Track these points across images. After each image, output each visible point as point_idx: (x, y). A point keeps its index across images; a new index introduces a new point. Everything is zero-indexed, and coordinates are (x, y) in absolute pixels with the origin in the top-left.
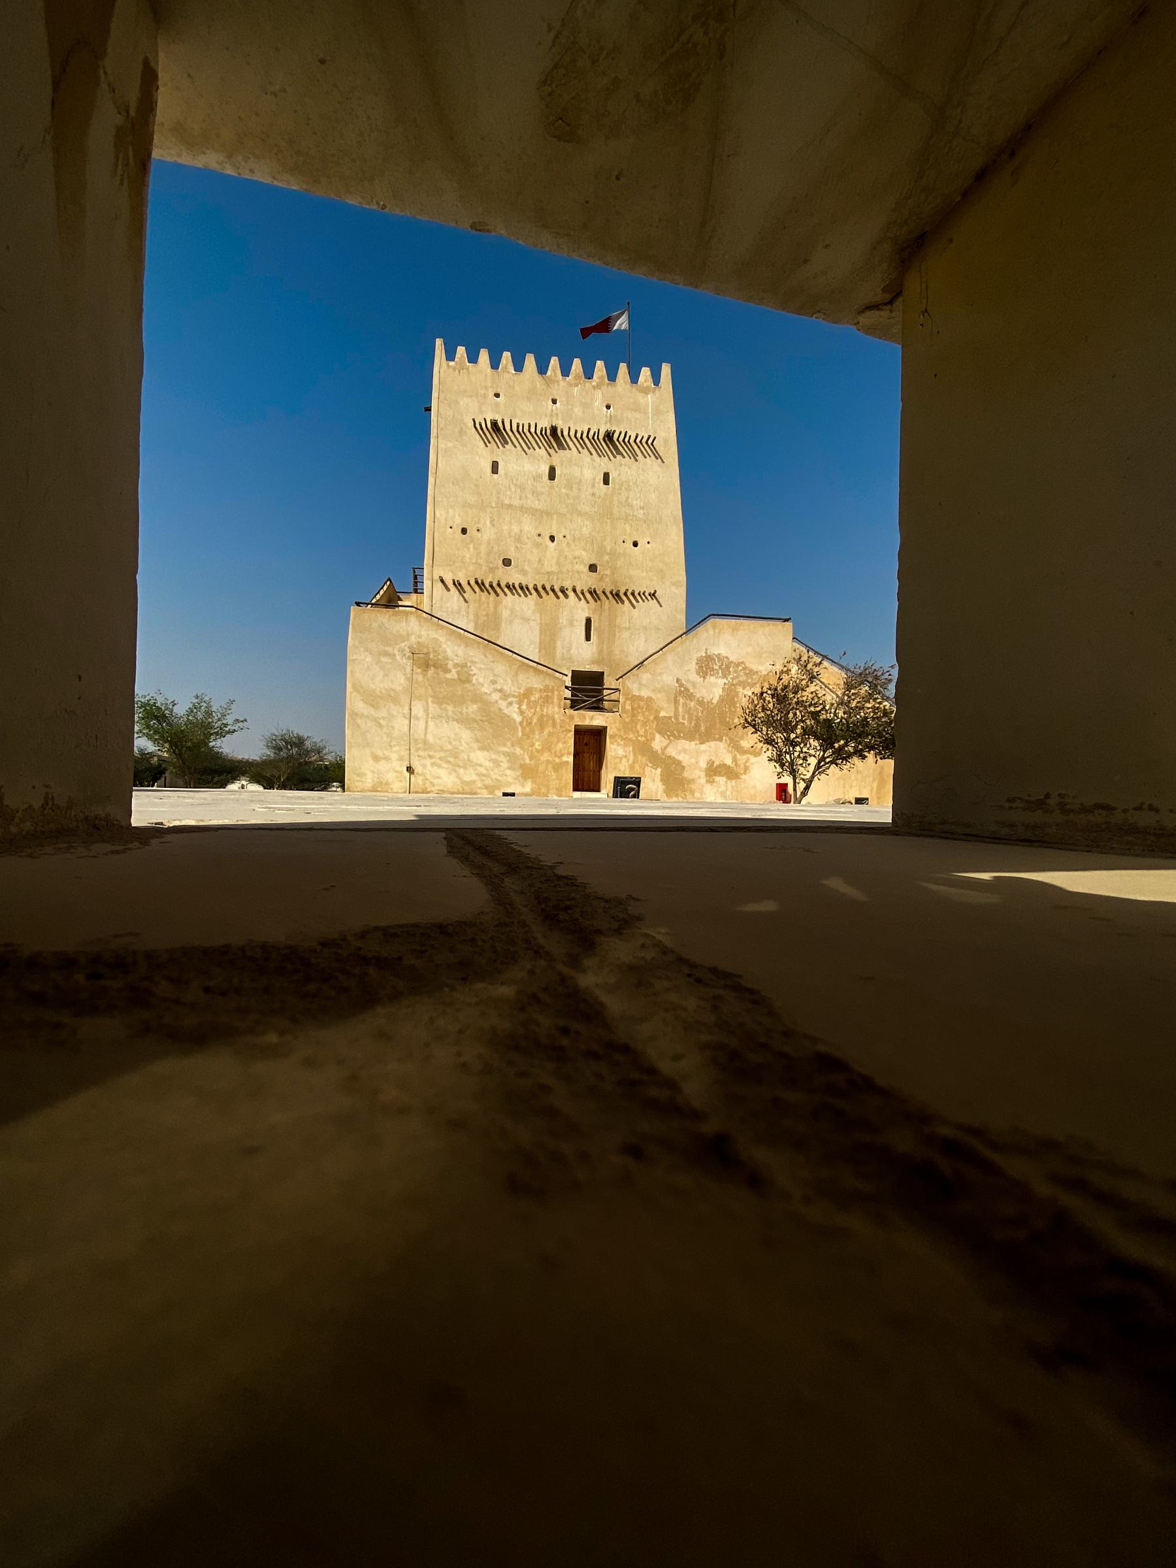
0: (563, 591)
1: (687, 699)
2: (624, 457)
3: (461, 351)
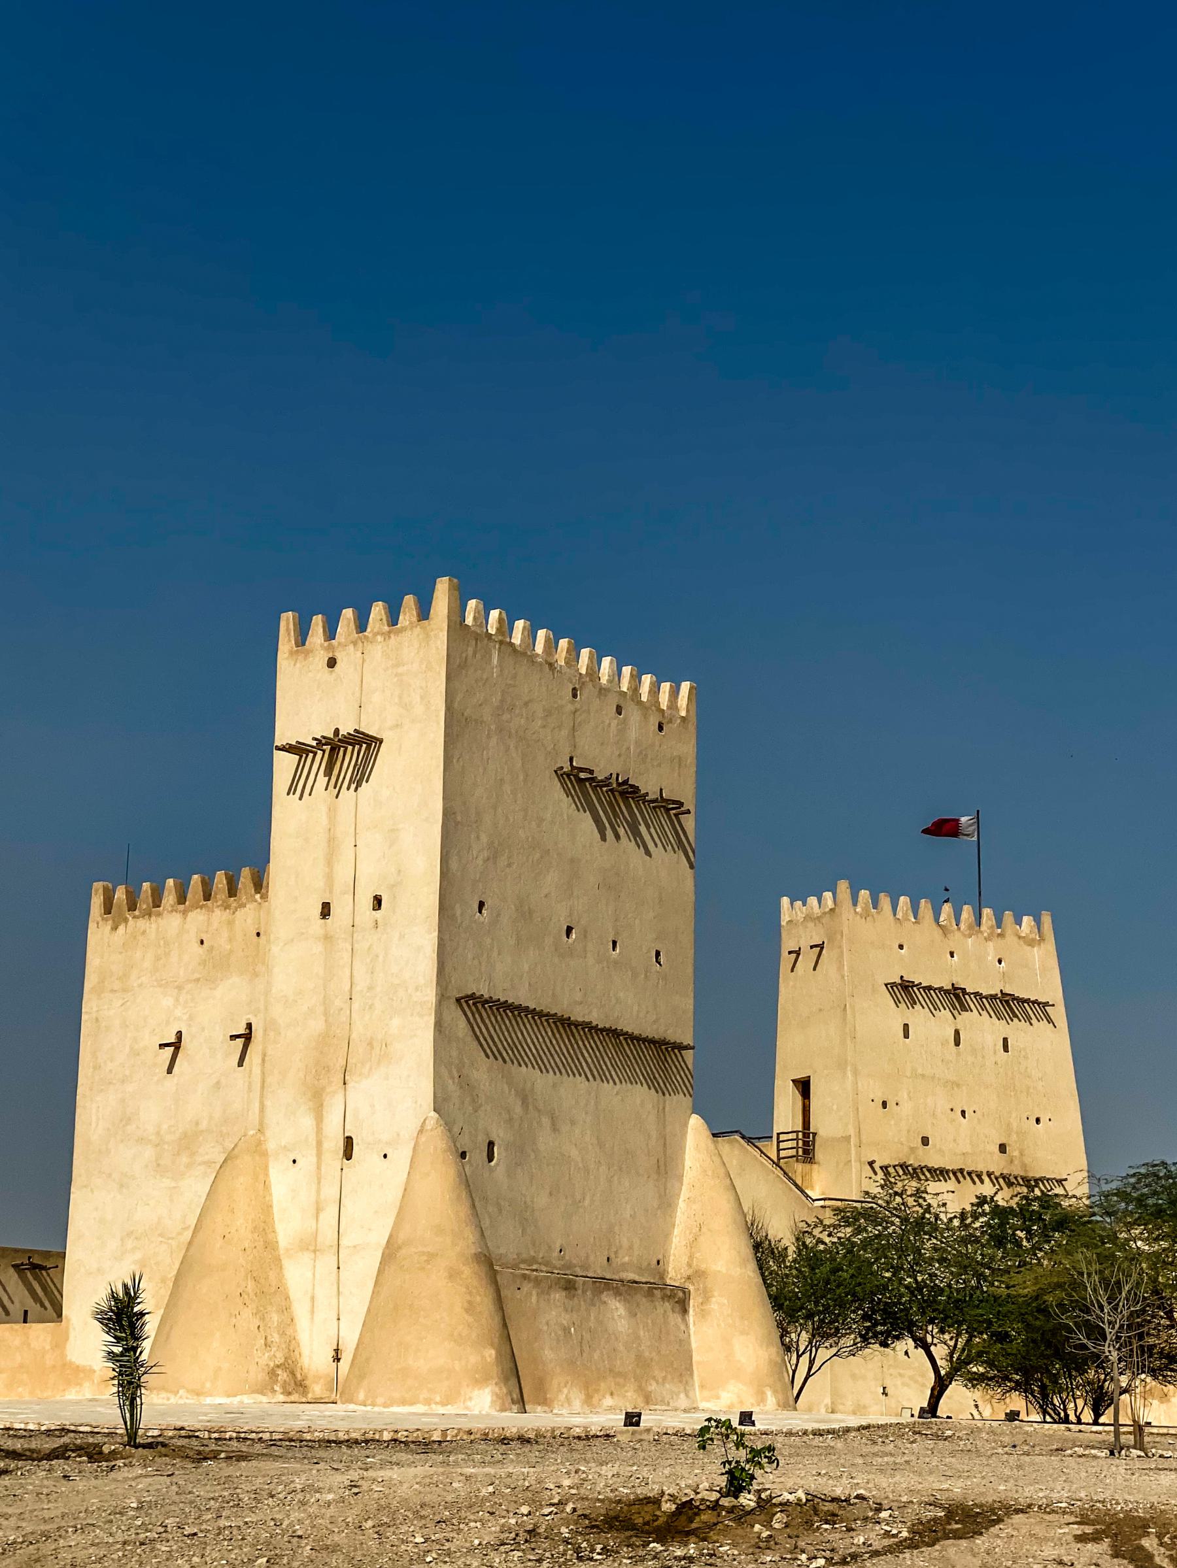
0: (979, 1176)
2: (1020, 1021)
3: (864, 894)
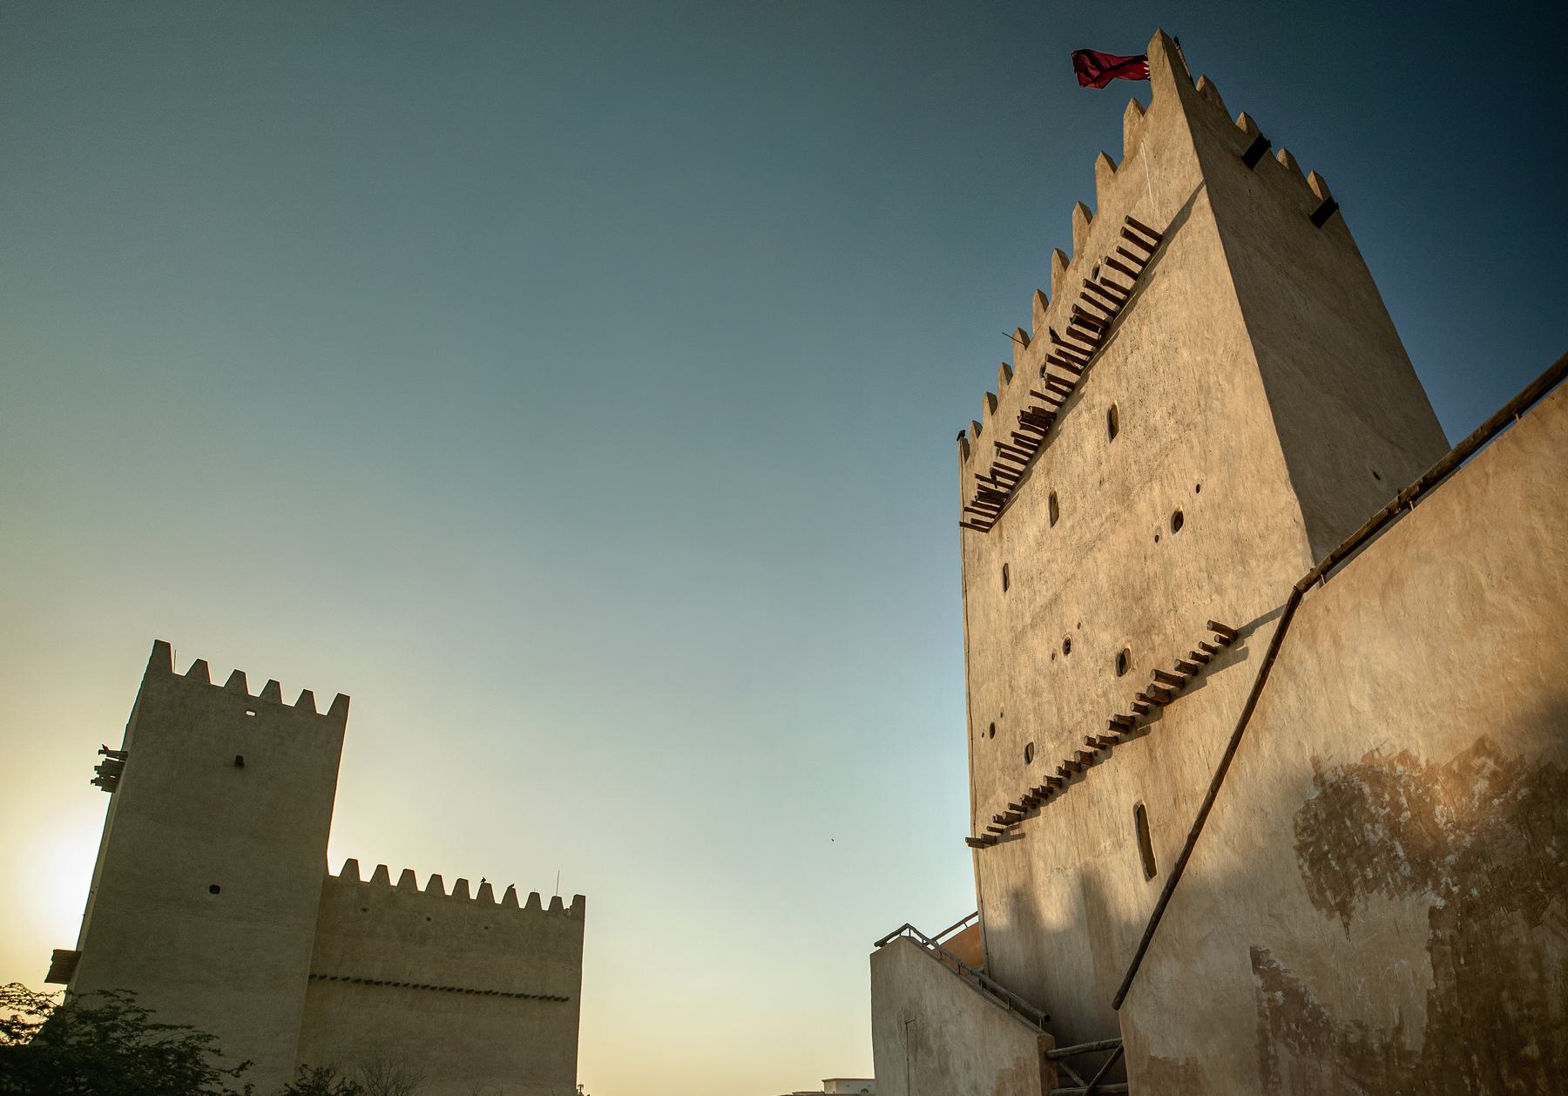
1: (1303, 1046)
